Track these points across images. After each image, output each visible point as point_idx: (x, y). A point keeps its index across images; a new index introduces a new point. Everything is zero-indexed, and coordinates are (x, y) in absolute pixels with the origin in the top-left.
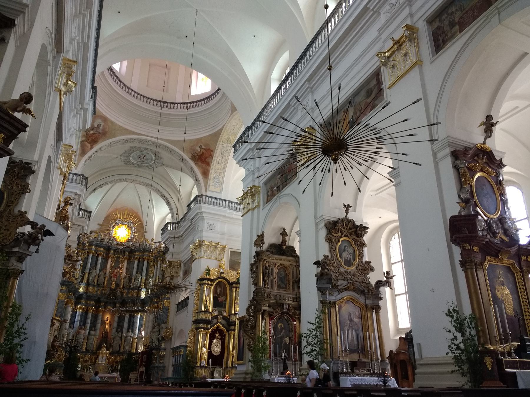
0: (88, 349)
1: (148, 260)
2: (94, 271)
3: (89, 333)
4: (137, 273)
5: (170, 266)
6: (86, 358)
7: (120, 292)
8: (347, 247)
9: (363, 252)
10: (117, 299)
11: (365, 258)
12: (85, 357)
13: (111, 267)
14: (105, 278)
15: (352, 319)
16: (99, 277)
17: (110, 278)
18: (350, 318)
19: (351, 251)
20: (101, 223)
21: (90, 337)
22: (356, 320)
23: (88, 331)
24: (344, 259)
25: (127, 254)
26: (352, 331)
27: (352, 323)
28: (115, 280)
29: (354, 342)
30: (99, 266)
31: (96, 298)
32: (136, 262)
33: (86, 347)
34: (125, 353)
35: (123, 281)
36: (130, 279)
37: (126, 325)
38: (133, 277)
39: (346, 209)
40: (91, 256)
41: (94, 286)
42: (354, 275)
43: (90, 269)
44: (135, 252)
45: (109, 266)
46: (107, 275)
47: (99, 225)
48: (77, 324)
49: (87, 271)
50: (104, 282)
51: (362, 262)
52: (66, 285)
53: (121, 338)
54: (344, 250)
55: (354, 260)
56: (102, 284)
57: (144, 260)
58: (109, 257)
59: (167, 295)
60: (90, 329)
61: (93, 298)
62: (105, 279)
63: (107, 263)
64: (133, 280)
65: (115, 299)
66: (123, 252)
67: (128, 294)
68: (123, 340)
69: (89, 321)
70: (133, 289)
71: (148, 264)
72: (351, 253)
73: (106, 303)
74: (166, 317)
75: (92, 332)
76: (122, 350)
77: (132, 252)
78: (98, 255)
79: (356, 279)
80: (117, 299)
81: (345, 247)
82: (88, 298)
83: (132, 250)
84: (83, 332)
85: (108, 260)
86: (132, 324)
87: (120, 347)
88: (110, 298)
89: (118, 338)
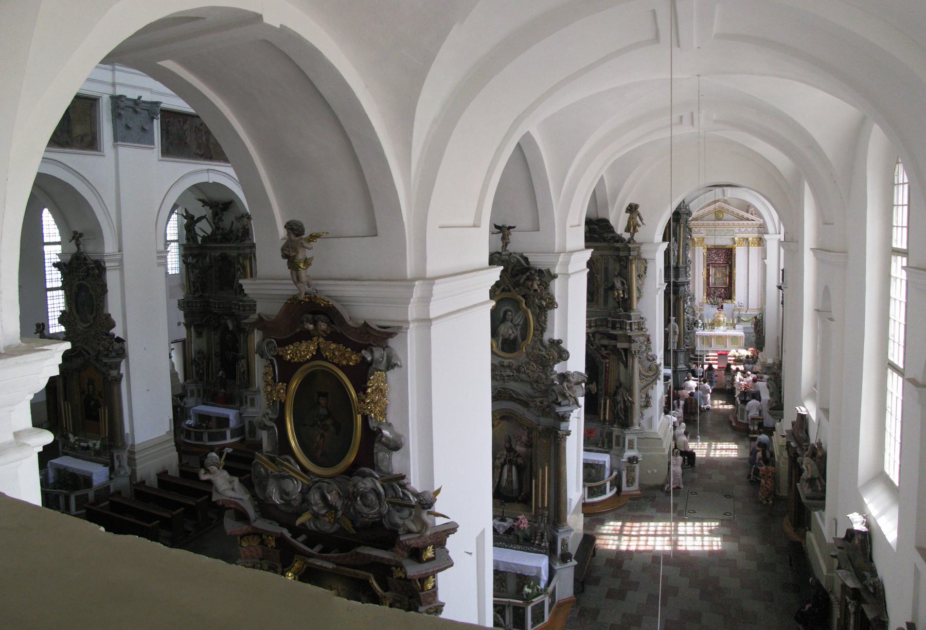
8: (510, 313)
9: (546, 321)
11: (553, 332)
15: (513, 446)
18: (508, 445)
19: (519, 320)
22: (520, 449)
24: (501, 338)
26: (511, 468)
27: (512, 454)
29: (512, 485)
39: (501, 235)
42: (518, 370)
51: (541, 341)
54: (504, 320)
55: (524, 337)
72: (518, 325)
79: (523, 376)
81: (505, 313)
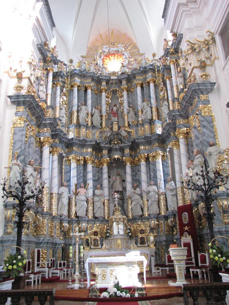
0: (96, 216)
1: (155, 82)
2: (84, 107)
3: (94, 194)
4: (143, 101)
5: (193, 49)
6: (95, 229)
7: (126, 131)
10: (124, 143)
12: (94, 227)
13: (108, 104)
14: (101, 116)
16: (92, 116)
17: (109, 119)
20: (85, 55)
21: (96, 199)
23: (90, 192)
25: (124, 82)
28: (117, 120)
30: (89, 102)
31: (94, 143)
32: (139, 89)
33: (94, 213)
34: (152, 216)
35: (126, 118)
36: (136, 114)
37: (144, 177)
38: (140, 109)
40: (76, 89)
41: (87, 127)
43: (78, 107)
44: (134, 77)
45: (104, 102)
46: (104, 114)
47: (82, 57)
48: (74, 181)
49: (75, 109)
50: (101, 124)
52: (24, 103)
53: (141, 196)
56: (99, 124)
57: (149, 83)
58: (101, 92)
59: (203, 97)
60: (95, 188)
61: (89, 143)
62: (101, 119)
63: (101, 99)
64: (140, 113)
65: (122, 143)
66: (119, 82)
67: (137, 133)
68: (145, 199)
69: (90, 176)
70: (143, 125)
71: (156, 86)
73: (110, 150)
74: (212, 135)
75: (98, 192)
76: (146, 214)
77: (130, 78)
78: (86, 91)
80: (124, 143)
82: (83, 144)
83: (129, 75)
84: (82, 191)
85: (101, 96)
86: (152, 174)
87: (142, 210)
88: (114, 143)
89: (138, 197)
